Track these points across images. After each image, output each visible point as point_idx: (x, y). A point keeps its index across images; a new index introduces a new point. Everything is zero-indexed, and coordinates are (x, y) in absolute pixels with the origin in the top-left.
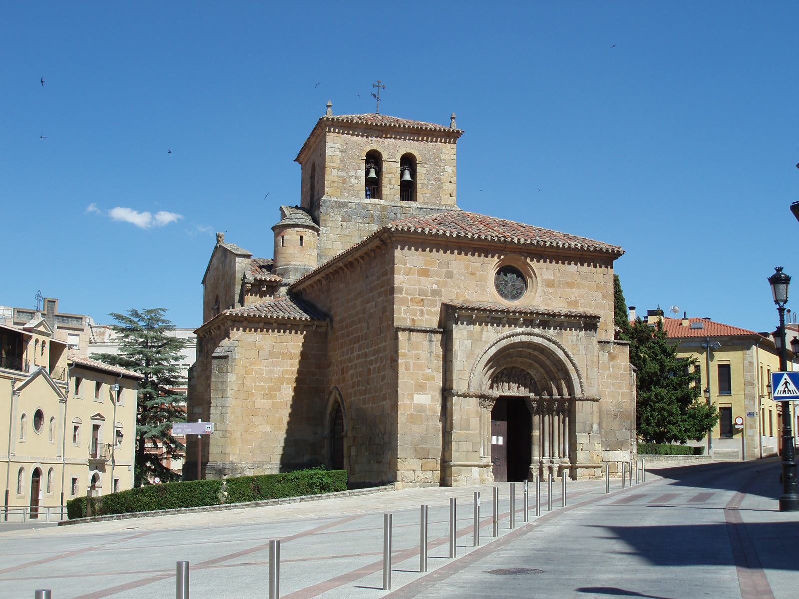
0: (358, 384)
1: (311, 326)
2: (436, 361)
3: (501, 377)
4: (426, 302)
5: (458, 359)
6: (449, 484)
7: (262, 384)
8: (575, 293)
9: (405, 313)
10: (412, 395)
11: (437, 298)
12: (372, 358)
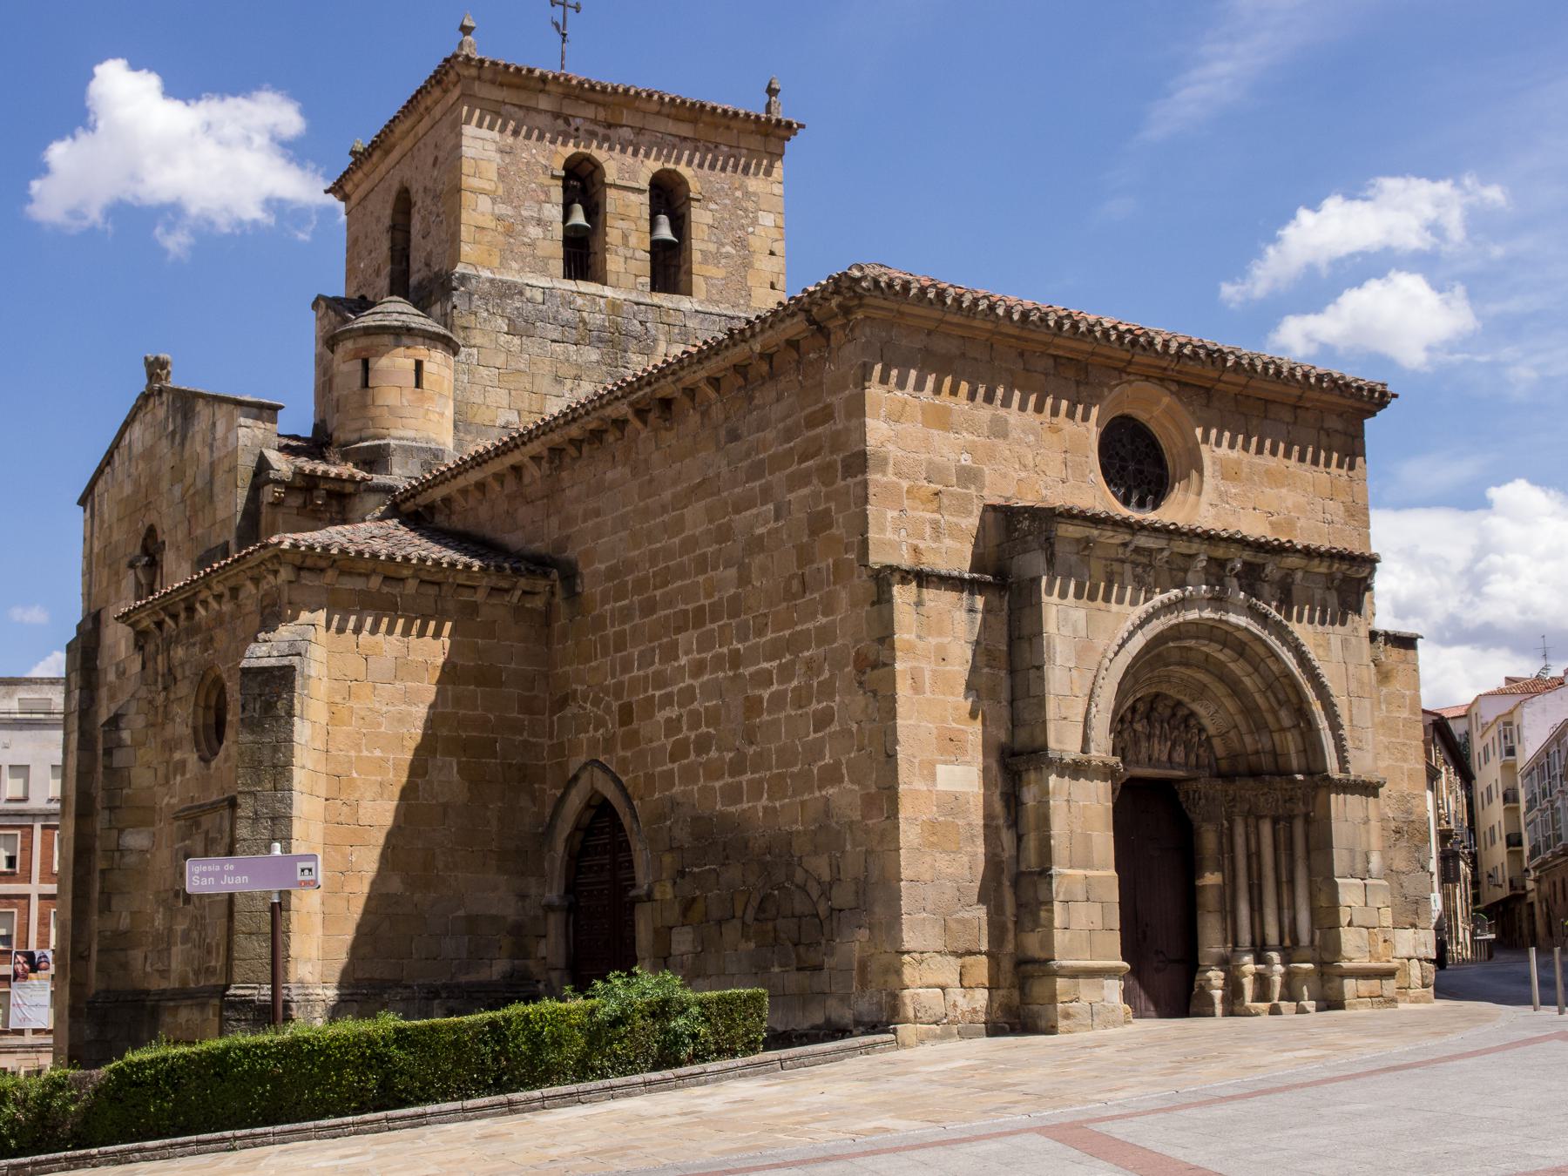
0: (703, 745)
1: (507, 591)
2: (986, 670)
4: (945, 501)
5: (1059, 661)
6: (1042, 1024)
7: (378, 753)
8: (1287, 499)
9: (897, 530)
10: (933, 764)
11: (972, 491)
12: (766, 665)
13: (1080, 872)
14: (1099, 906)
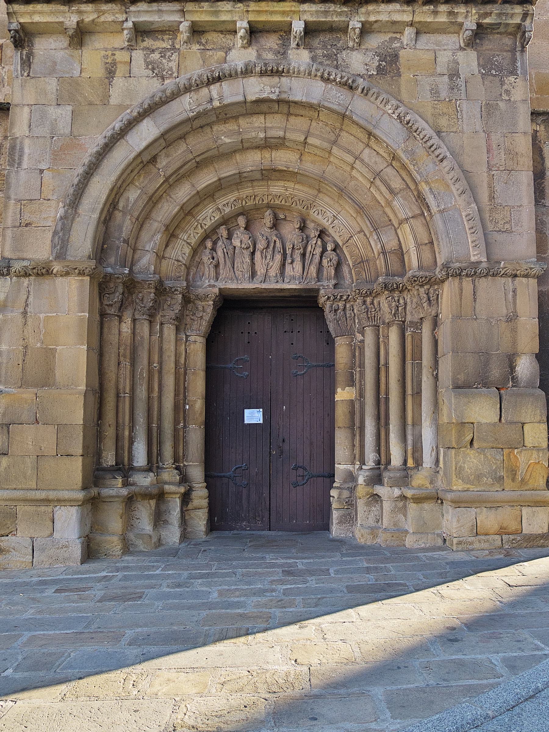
3: (230, 238)
13: (28, 394)
14: (51, 430)
